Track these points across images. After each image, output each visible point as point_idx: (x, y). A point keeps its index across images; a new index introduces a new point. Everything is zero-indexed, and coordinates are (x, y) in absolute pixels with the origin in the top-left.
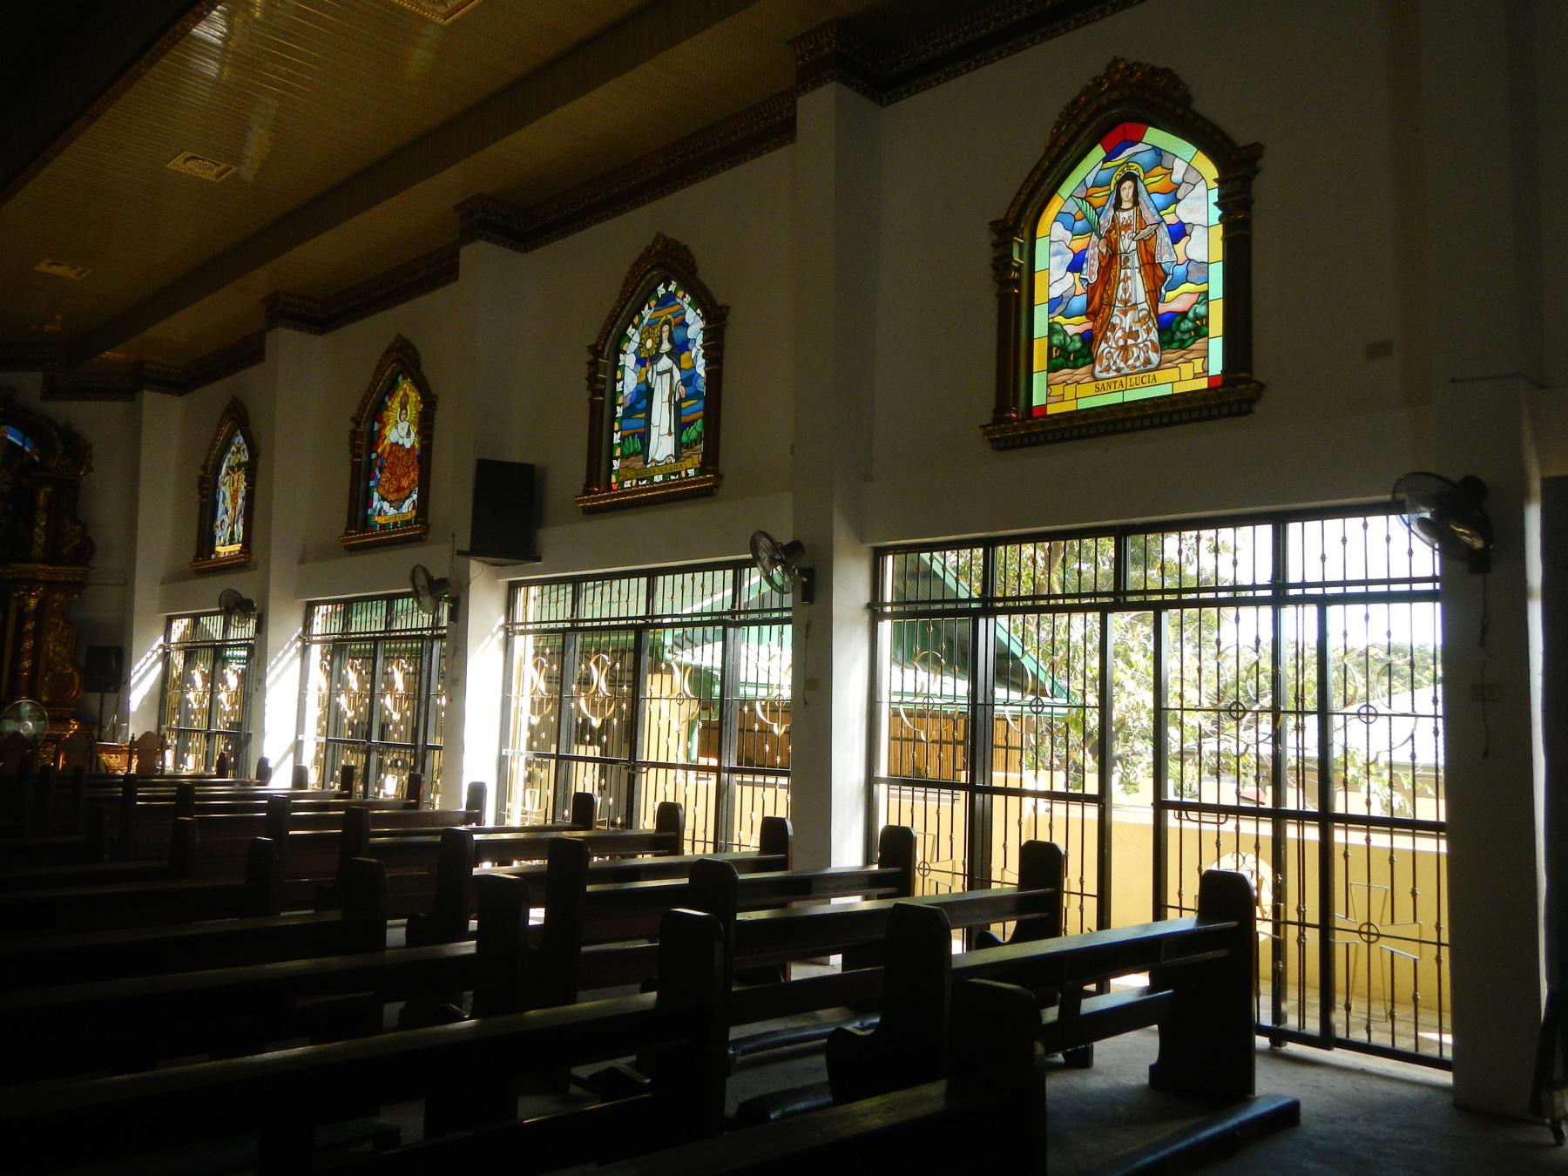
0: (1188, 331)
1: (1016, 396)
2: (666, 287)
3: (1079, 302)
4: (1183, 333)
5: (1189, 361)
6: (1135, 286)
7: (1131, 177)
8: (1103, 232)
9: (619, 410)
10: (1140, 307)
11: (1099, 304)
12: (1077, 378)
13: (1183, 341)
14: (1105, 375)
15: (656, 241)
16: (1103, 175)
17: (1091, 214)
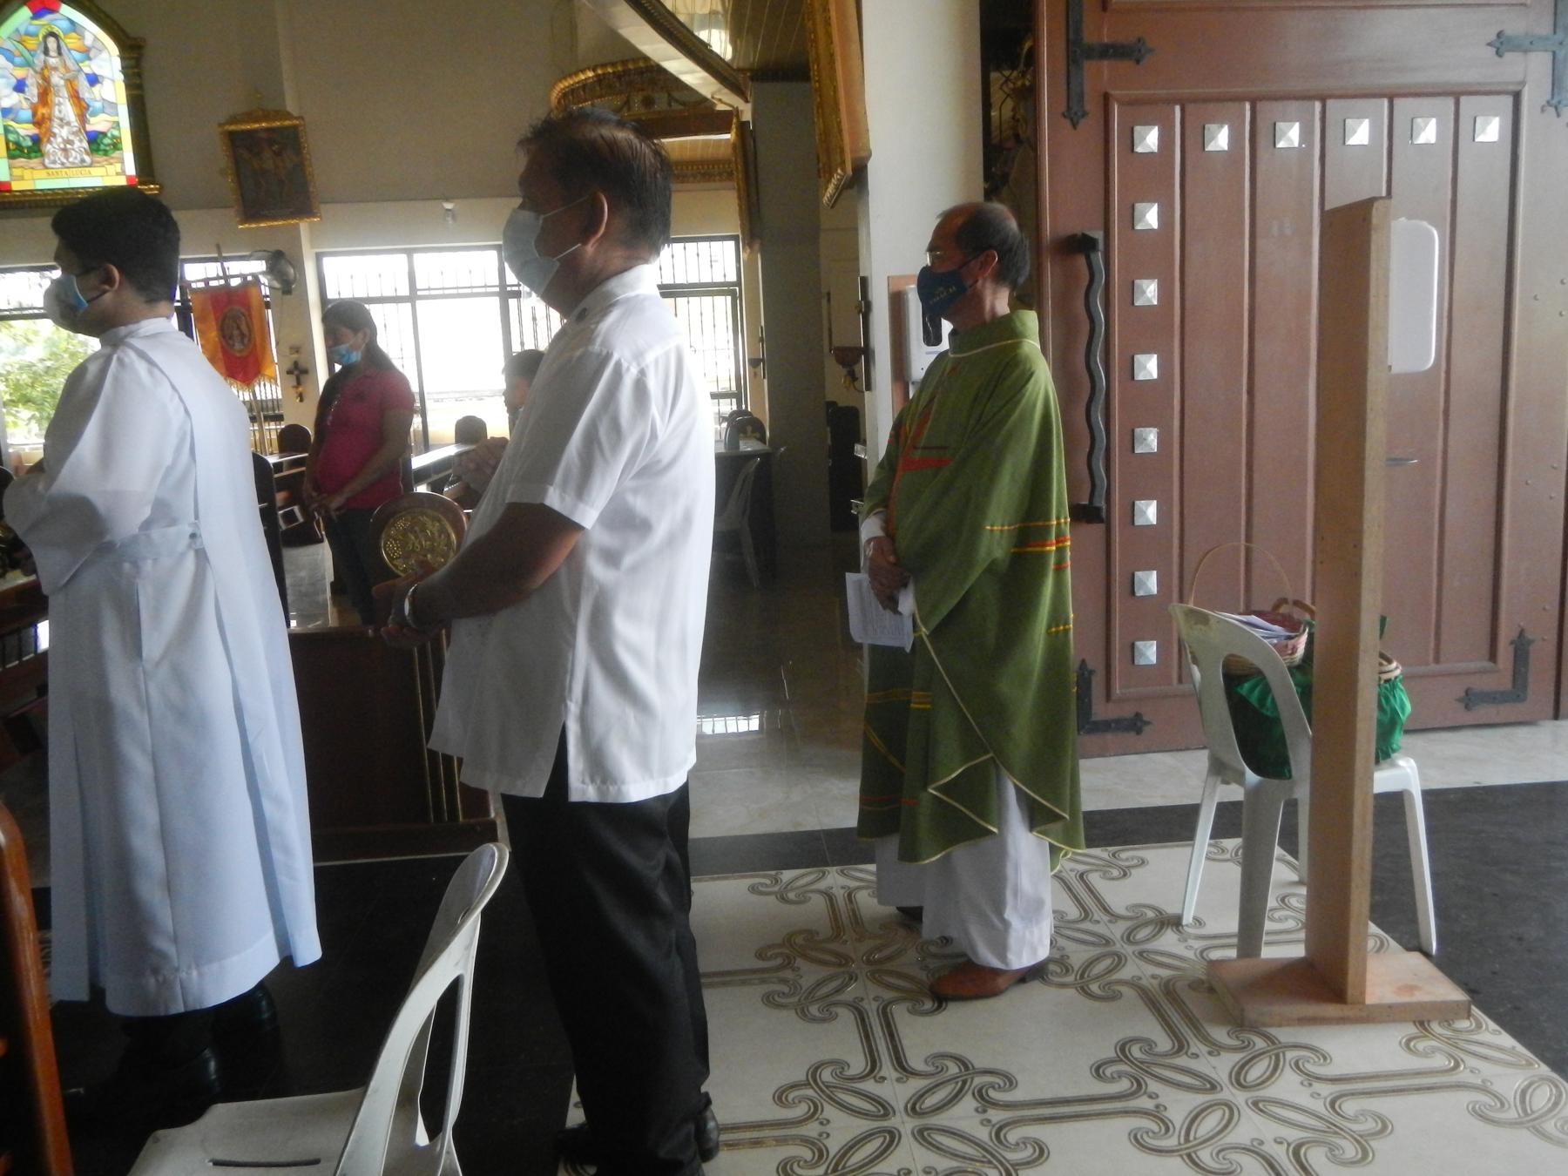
0: (109, 145)
3: (26, 114)
4: (106, 145)
5: (111, 164)
8: (38, 69)
10: (72, 124)
12: (32, 165)
14: (52, 166)
16: (32, 29)
17: (27, 54)
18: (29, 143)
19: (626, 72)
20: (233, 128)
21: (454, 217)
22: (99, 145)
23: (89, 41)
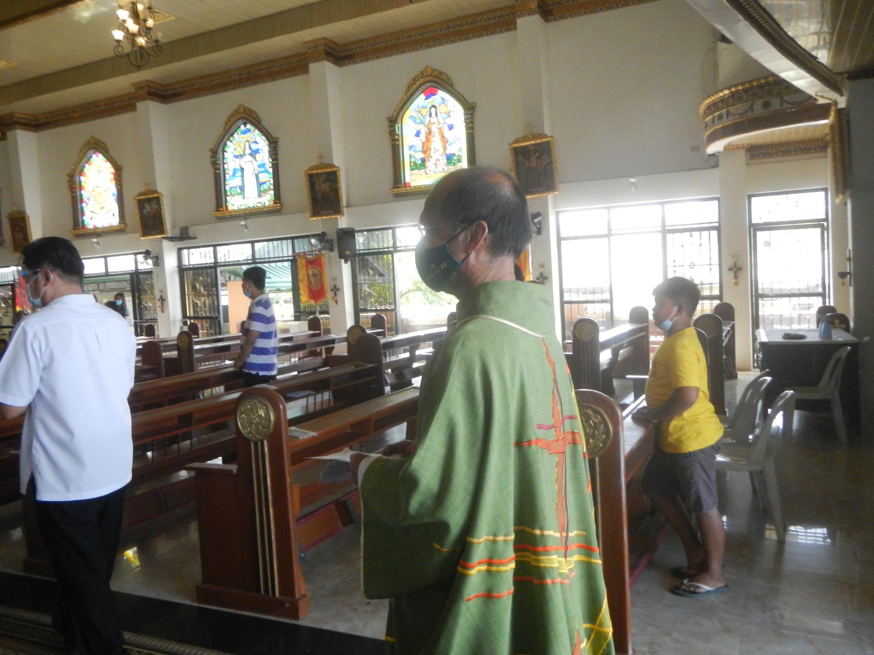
0: (456, 160)
1: (401, 180)
2: (245, 126)
3: (420, 148)
6: (436, 143)
7: (434, 106)
8: (426, 124)
9: (227, 177)
11: (426, 150)
12: (420, 173)
13: (454, 163)
15: (239, 107)
16: (425, 105)
18: (420, 162)
19: (752, 88)
20: (516, 145)
21: (636, 187)
22: (451, 160)
23: (450, 108)
